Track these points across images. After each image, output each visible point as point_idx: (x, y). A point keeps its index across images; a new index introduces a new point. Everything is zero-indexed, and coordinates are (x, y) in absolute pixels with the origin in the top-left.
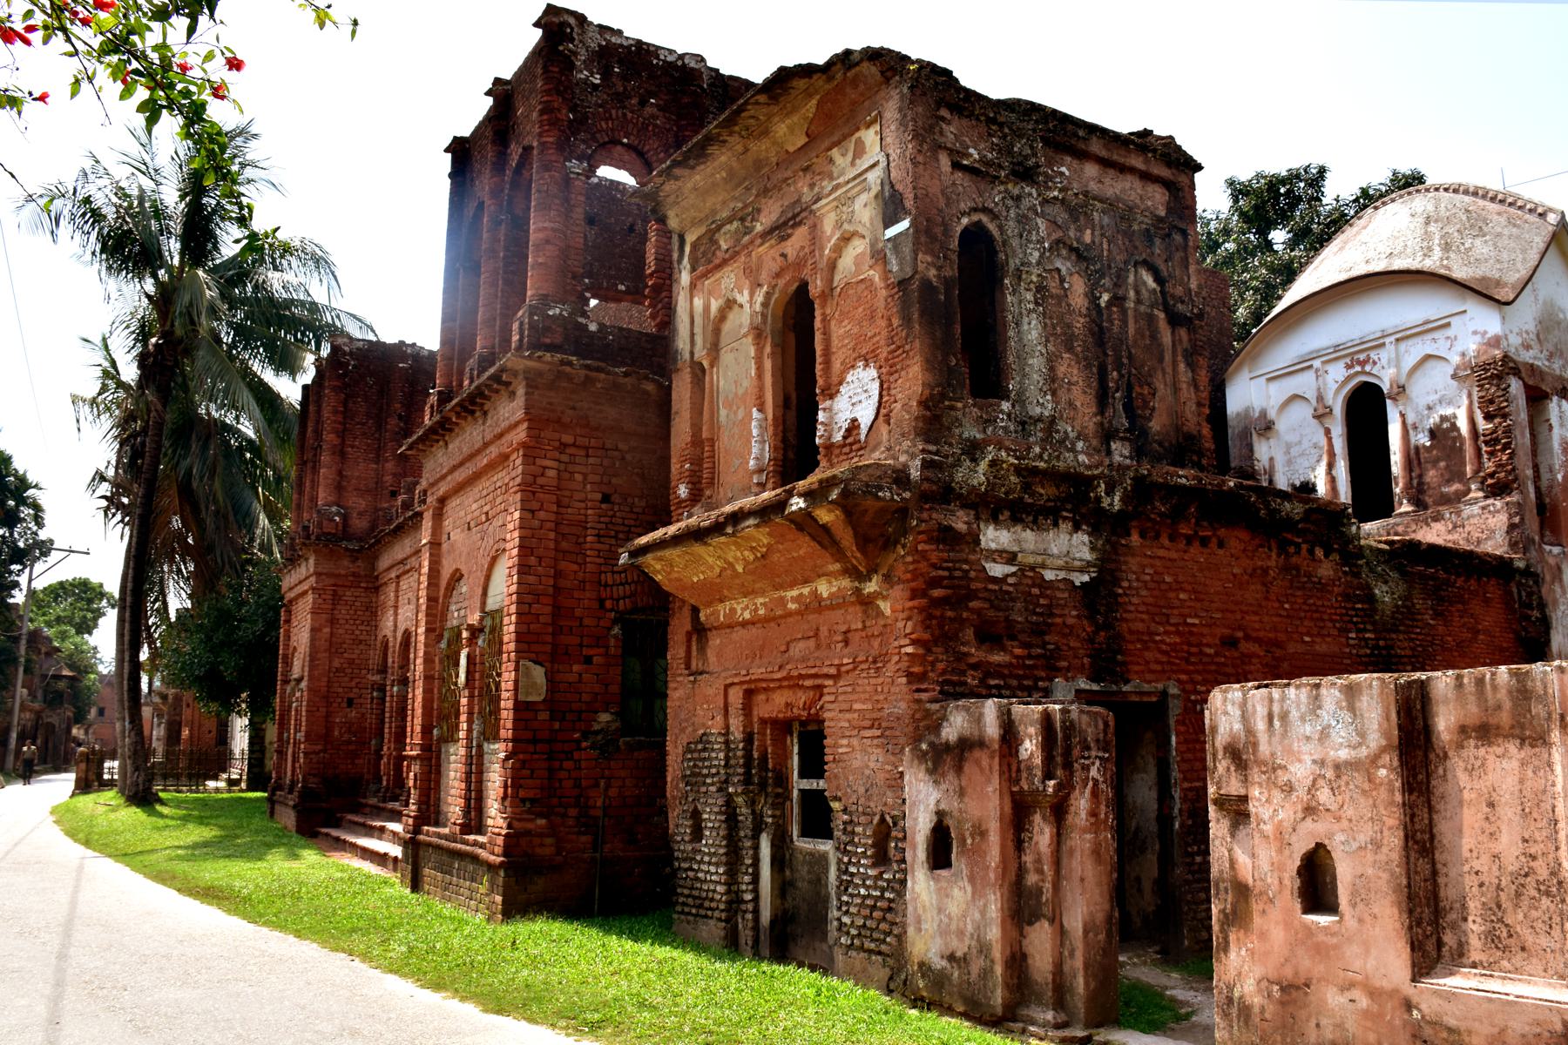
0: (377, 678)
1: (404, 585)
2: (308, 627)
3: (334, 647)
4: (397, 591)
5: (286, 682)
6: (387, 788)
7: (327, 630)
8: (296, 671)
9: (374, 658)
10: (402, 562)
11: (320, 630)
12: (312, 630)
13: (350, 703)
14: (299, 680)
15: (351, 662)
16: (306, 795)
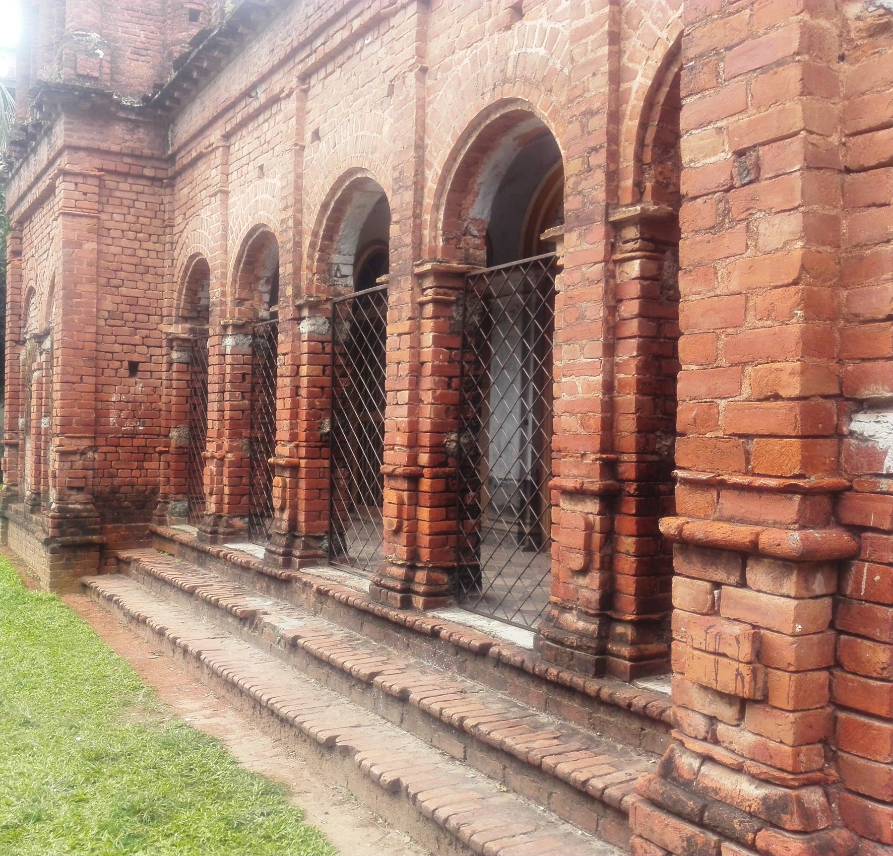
0: (178, 330)
1: (244, 145)
2: (59, 241)
3: (105, 276)
4: (226, 163)
5: (20, 342)
6: (218, 517)
7: (90, 246)
8: (35, 324)
9: (172, 295)
10: (248, 93)
11: (79, 245)
12: (67, 243)
13: (133, 368)
14: (47, 333)
15: (133, 302)
16: (65, 521)
